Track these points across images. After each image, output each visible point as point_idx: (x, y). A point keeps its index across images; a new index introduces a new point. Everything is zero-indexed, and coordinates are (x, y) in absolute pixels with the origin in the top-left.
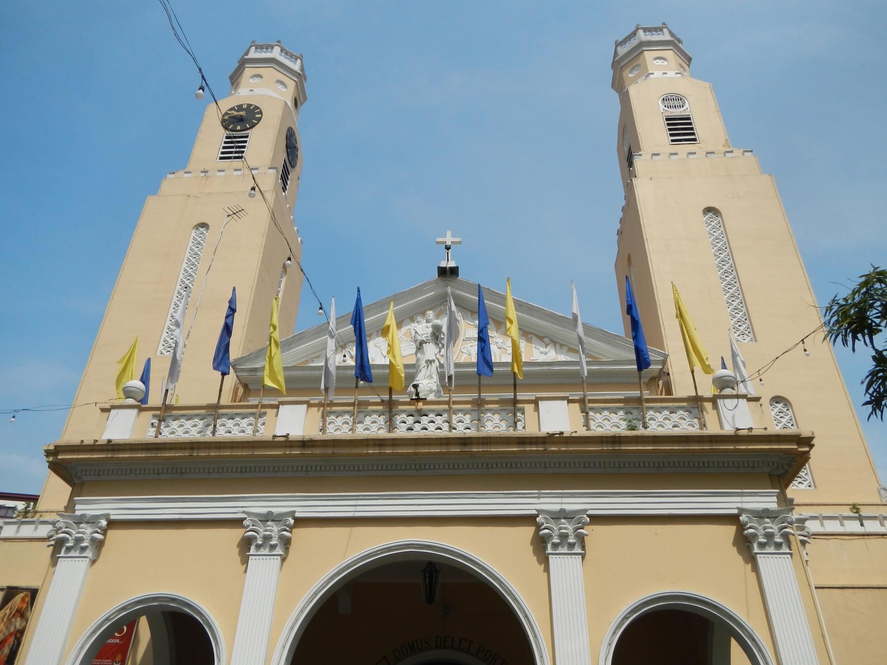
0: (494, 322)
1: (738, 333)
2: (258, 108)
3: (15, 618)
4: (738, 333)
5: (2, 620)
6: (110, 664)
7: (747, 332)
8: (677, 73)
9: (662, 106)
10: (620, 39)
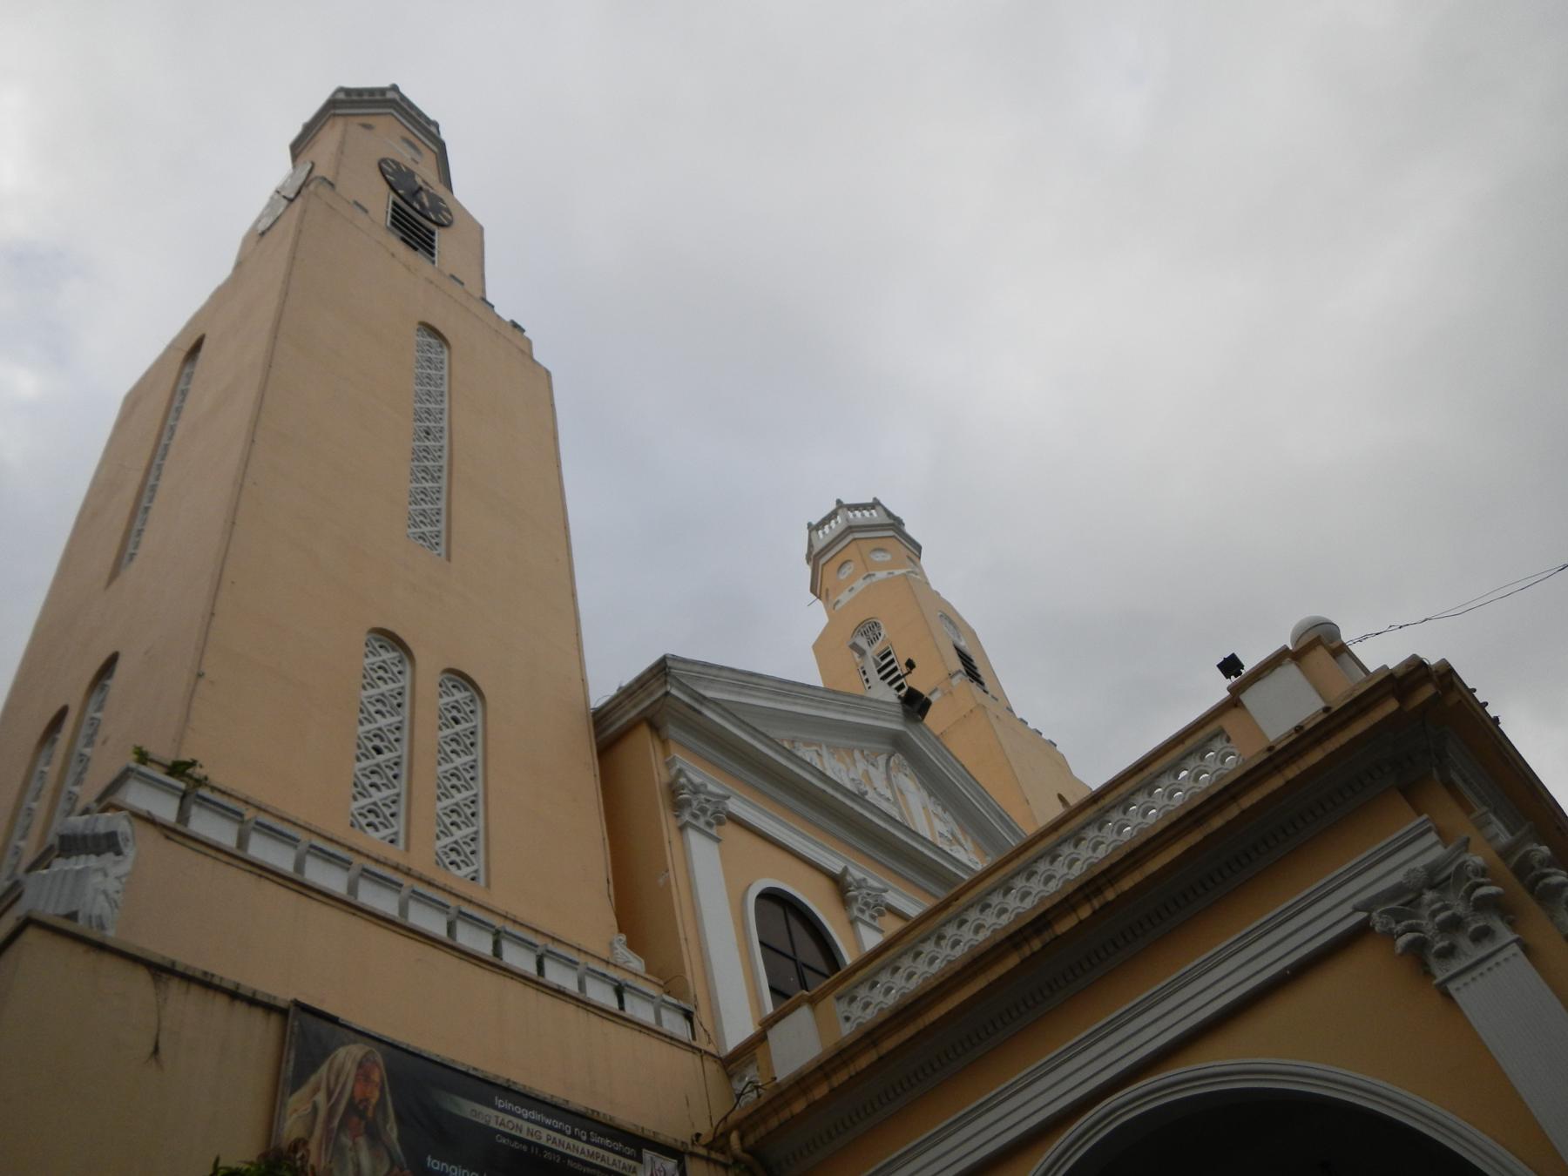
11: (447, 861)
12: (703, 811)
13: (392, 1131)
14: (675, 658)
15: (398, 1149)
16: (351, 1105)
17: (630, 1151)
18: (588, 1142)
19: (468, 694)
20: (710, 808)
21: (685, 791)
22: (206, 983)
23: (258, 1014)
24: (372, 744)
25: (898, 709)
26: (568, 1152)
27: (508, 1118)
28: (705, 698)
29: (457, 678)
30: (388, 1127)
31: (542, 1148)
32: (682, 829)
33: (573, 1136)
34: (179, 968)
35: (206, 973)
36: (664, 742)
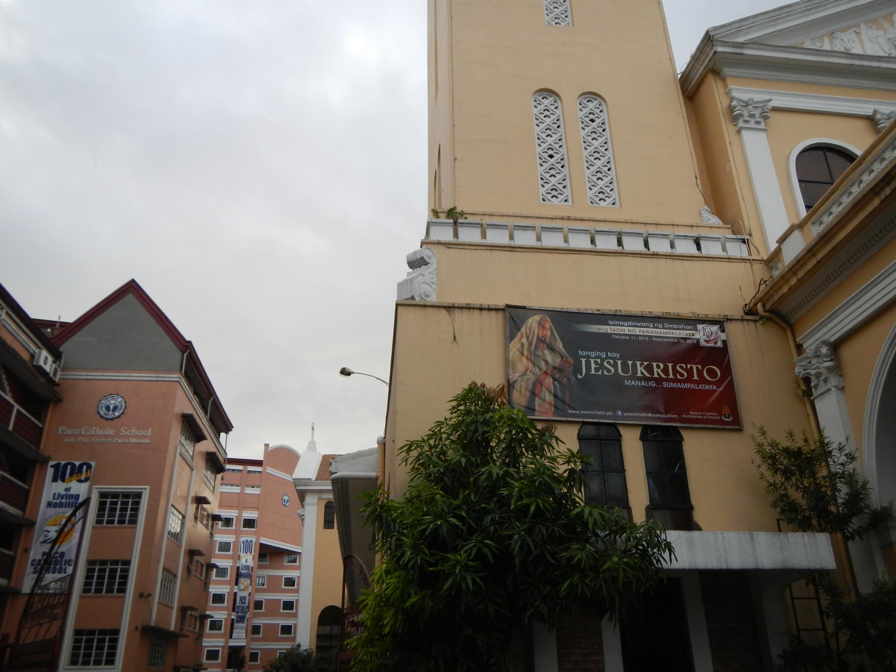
3: (539, 350)
6: (716, 418)
11: (597, 200)
12: (752, 116)
13: (560, 345)
15: (564, 351)
16: (538, 339)
18: (663, 328)
19: (597, 102)
20: (757, 113)
21: (736, 109)
22: (469, 308)
23: (493, 313)
24: (547, 154)
26: (652, 334)
27: (616, 327)
28: (743, 43)
29: (588, 96)
30: (557, 344)
31: (637, 336)
32: (739, 132)
33: (654, 327)
34: (456, 305)
35: (467, 304)
36: (724, 80)
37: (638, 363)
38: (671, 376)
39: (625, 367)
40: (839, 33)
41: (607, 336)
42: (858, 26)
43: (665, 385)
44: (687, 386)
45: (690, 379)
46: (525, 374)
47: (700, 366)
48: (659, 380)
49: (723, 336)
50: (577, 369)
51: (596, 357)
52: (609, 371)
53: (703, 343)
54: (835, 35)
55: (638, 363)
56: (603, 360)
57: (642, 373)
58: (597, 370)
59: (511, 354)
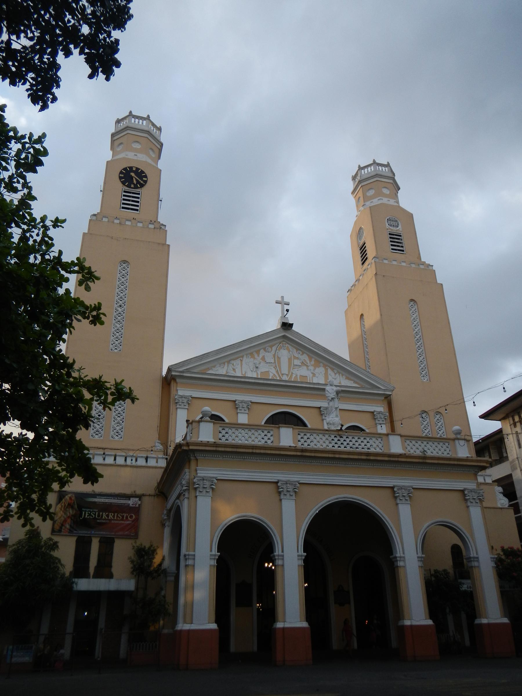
0: (308, 357)
1: (422, 375)
2: (144, 173)
4: (422, 375)
5: (61, 510)
7: (425, 375)
8: (395, 202)
9: (387, 225)
10: (362, 166)
13: (76, 506)
14: (172, 366)
17: (127, 499)
18: (117, 499)
24: (98, 415)
25: (281, 329)
32: (177, 408)
33: (114, 499)
37: (104, 513)
38: (115, 518)
39: (99, 516)
40: (232, 361)
41: (95, 502)
42: (243, 357)
43: (112, 522)
44: (121, 522)
45: (122, 520)
46: (60, 518)
47: (127, 514)
48: (111, 520)
49: (139, 502)
50: (81, 515)
51: (89, 511)
52: (92, 516)
53: (131, 505)
54: (230, 362)
55: (104, 513)
56: (91, 512)
57: (105, 517)
58: (88, 516)
59: (57, 510)
